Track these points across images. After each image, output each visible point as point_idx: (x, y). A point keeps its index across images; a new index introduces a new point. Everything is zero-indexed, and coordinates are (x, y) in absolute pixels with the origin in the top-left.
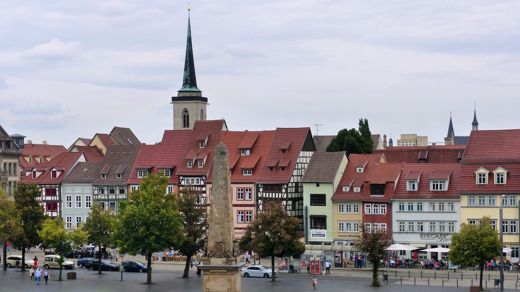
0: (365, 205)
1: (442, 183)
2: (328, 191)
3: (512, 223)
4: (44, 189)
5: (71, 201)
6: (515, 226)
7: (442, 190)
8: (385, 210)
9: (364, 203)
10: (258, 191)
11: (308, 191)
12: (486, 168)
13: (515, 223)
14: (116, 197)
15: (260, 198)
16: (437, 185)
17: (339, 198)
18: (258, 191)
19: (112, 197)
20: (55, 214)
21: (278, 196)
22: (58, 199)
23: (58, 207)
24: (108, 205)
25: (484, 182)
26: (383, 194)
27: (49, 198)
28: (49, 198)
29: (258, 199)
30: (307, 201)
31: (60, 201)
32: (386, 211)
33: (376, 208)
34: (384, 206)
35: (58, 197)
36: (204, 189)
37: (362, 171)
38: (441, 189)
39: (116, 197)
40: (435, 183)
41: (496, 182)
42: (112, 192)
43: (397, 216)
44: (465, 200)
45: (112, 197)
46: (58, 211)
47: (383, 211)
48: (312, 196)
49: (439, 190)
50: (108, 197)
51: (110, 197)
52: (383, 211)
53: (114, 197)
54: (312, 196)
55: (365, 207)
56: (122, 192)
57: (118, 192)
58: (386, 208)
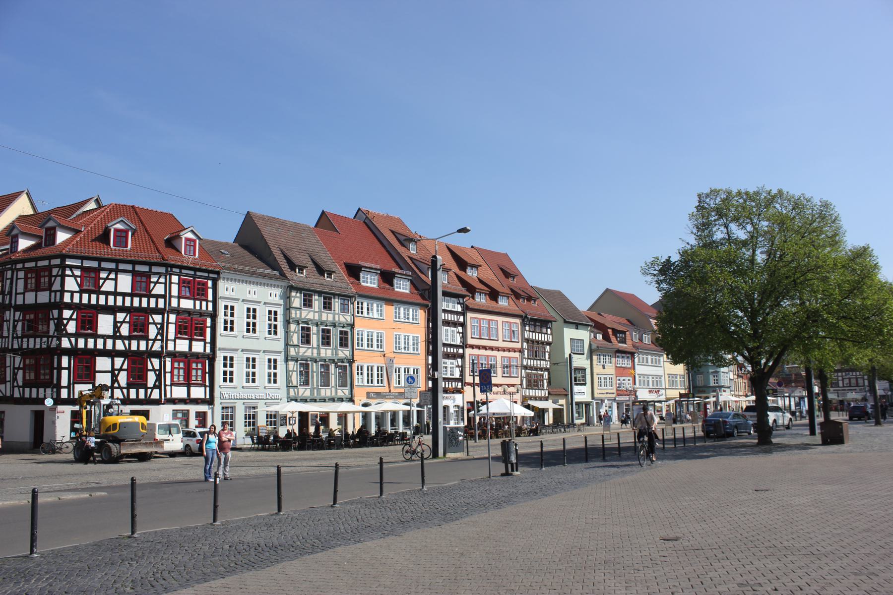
4: (175, 279)
5: (246, 320)
10: (523, 330)
14: (334, 318)
15: (527, 340)
18: (523, 330)
19: (327, 316)
20: (198, 347)
22: (210, 308)
23: (208, 330)
24: (318, 334)
28: (187, 304)
31: (214, 316)
35: (210, 305)
36: (461, 319)
39: (334, 318)
43: (640, 370)
45: (327, 316)
46: (208, 339)
50: (320, 316)
51: (324, 318)
53: (330, 318)
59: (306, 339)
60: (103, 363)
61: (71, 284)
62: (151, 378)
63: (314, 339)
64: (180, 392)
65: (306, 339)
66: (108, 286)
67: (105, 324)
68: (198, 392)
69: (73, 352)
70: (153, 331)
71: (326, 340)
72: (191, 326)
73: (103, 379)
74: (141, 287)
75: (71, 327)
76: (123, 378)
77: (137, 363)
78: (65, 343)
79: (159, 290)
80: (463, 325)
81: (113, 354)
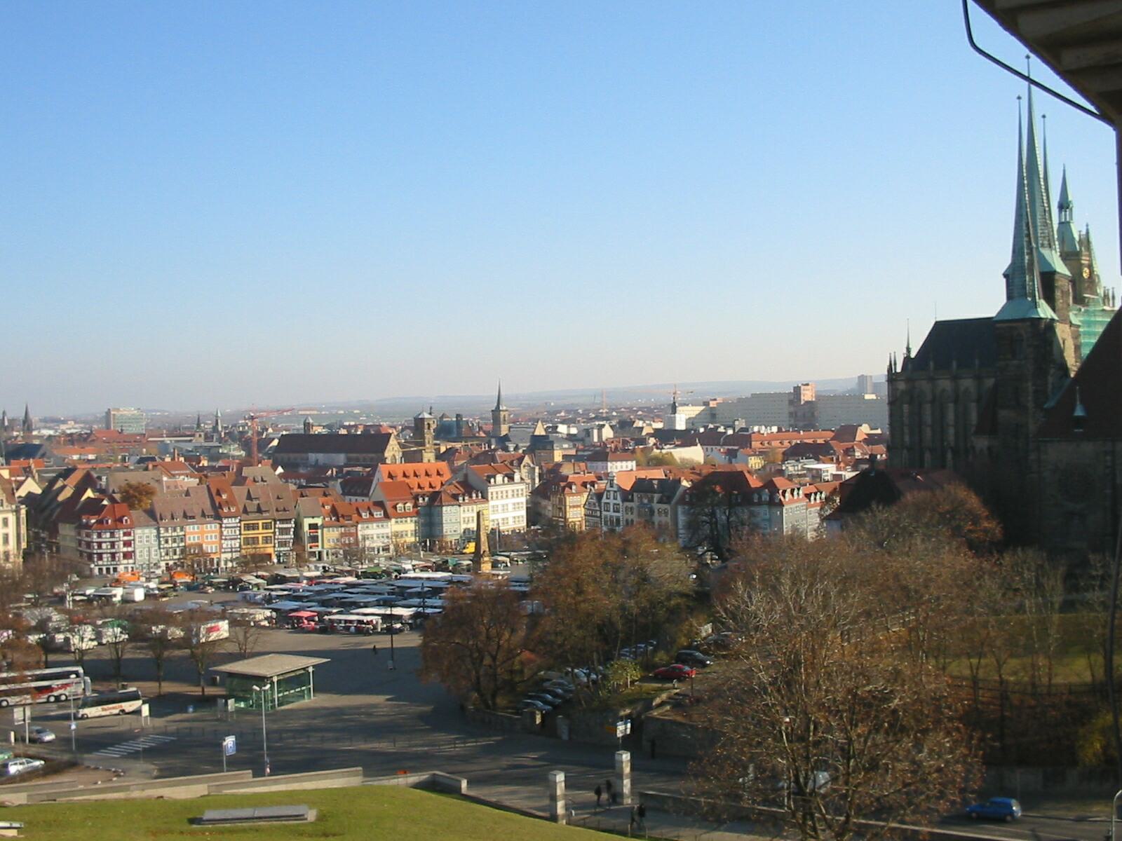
2: (319, 521)
10: (275, 524)
11: (307, 522)
15: (279, 528)
20: (130, 549)
21: (289, 526)
27: (126, 538)
29: (275, 528)
30: (306, 528)
31: (134, 540)
42: (175, 530)
44: (393, 520)
48: (310, 525)
54: (310, 525)
56: (182, 530)
57: (178, 530)
59: (167, 542)
60: (105, 556)
61: (95, 537)
62: (117, 559)
63: (170, 542)
64: (125, 561)
65: (167, 542)
66: (104, 536)
67: (104, 546)
68: (131, 561)
69: (97, 553)
70: (116, 547)
71: (174, 541)
72: (127, 544)
73: (105, 560)
74: (112, 535)
75: (96, 547)
76: (110, 559)
77: (113, 555)
78: (95, 551)
79: (117, 536)
80: (240, 527)
81: (107, 553)
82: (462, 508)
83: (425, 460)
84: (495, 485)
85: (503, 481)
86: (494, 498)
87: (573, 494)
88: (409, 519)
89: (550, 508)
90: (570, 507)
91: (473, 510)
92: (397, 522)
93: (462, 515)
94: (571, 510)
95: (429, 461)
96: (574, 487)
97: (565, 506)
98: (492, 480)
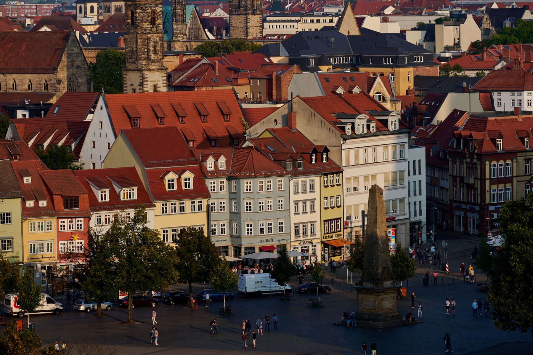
0: (60, 220)
1: (131, 191)
3: (173, 231)
6: (167, 235)
7: (132, 199)
8: (81, 225)
9: (58, 218)
12: (176, 172)
13: (167, 231)
16: (127, 193)
17: (27, 213)
25: (173, 188)
26: (78, 207)
32: (83, 226)
33: (71, 224)
34: (81, 221)
37: (30, 181)
38: (130, 197)
40: (125, 192)
41: (184, 188)
47: (79, 226)
49: (129, 199)
52: (79, 226)
55: (60, 224)
58: (82, 223)
82: (292, 183)
83: (149, 88)
84: (354, 136)
85: (368, 126)
86: (352, 163)
87: (496, 156)
88: (188, 204)
89: (446, 184)
90: (493, 182)
91: (312, 186)
92: (164, 211)
93: (294, 197)
94: (494, 187)
95: (155, 87)
96: (499, 143)
97: (483, 180)
98: (348, 127)
